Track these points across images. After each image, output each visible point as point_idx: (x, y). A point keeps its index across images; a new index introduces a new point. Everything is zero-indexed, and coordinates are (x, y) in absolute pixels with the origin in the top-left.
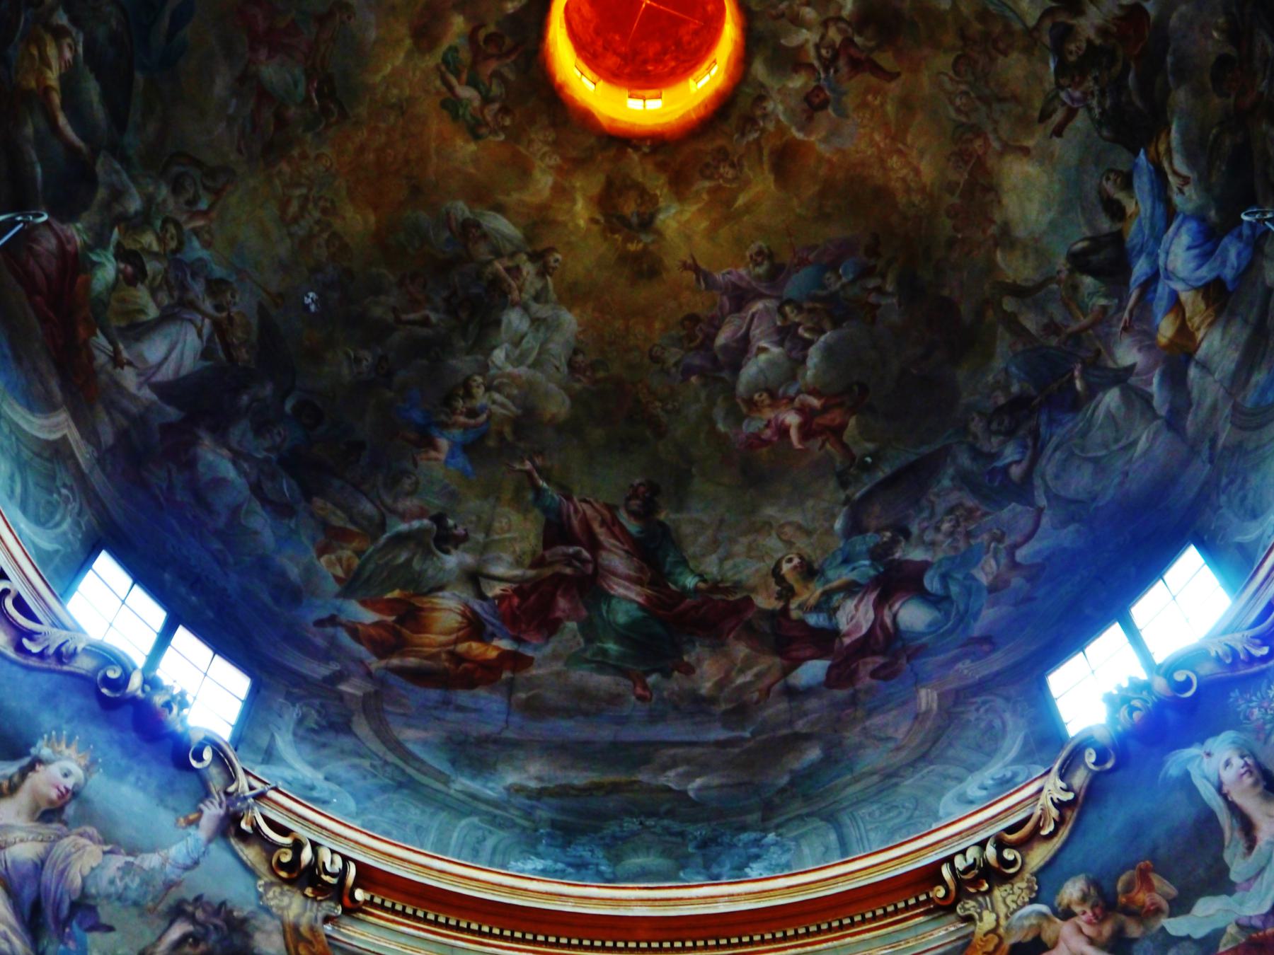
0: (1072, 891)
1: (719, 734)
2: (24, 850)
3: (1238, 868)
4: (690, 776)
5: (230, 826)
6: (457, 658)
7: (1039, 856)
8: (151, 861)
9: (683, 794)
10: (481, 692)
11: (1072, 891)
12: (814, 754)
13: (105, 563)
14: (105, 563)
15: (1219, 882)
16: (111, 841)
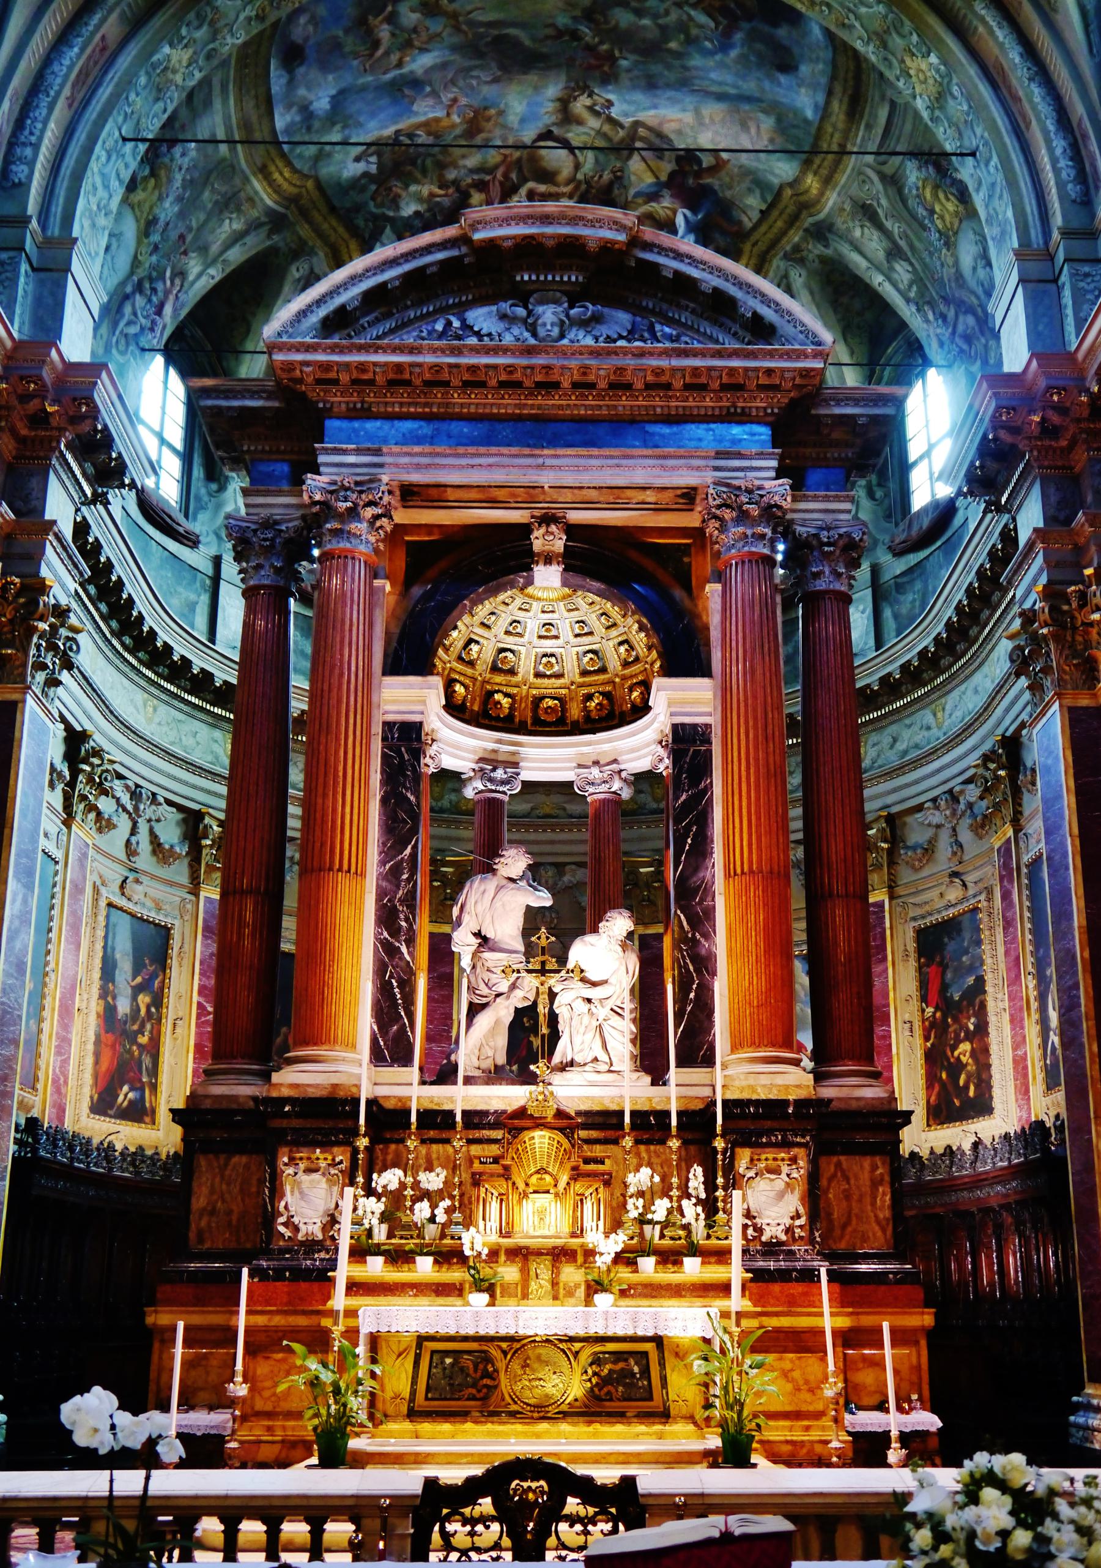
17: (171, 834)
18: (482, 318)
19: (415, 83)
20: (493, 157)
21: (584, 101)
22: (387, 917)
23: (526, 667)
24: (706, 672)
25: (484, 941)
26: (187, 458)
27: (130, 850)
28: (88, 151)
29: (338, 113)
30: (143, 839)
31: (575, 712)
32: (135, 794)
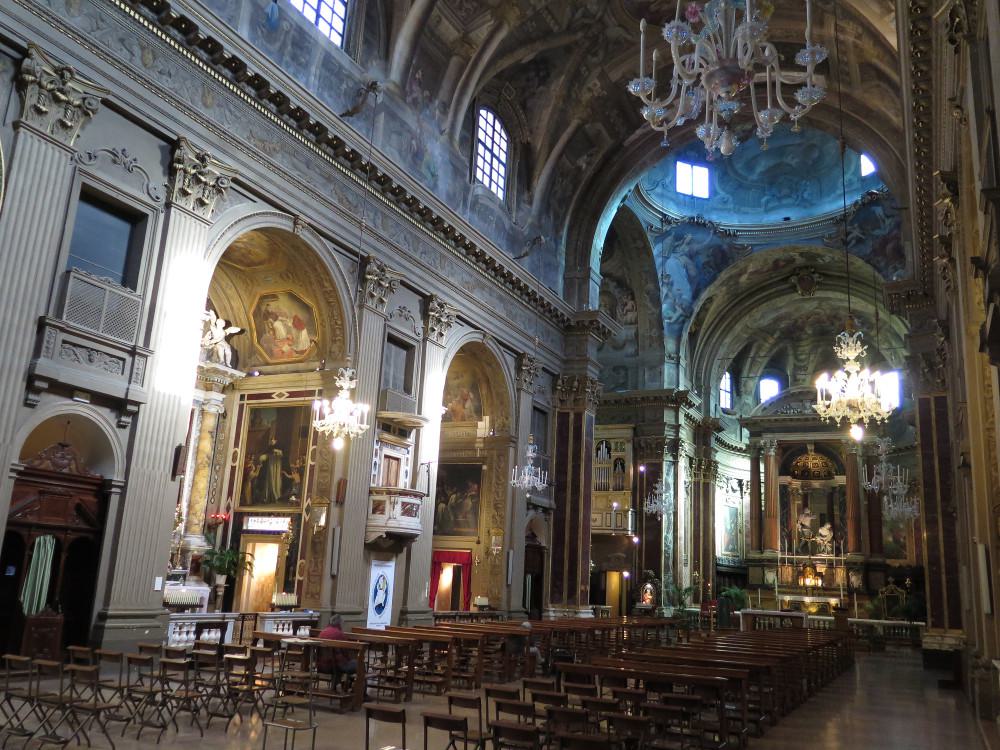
0: (856, 225)
1: (798, 141)
2: (687, 249)
3: (882, 226)
4: (793, 158)
5: (715, 233)
6: (744, 131)
7: (851, 218)
8: (705, 243)
9: (791, 165)
10: (750, 140)
11: (856, 225)
12: (816, 155)
13: (679, 163)
14: (679, 163)
15: (879, 228)
16: (699, 243)
17: (736, 487)
18: (793, 405)
19: (781, 308)
20: (803, 313)
21: (824, 304)
22: (782, 523)
23: (810, 465)
24: (844, 474)
25: (803, 526)
26: (731, 393)
27: (727, 492)
28: (712, 364)
29: (762, 317)
30: (730, 488)
31: (822, 474)
32: (728, 479)
